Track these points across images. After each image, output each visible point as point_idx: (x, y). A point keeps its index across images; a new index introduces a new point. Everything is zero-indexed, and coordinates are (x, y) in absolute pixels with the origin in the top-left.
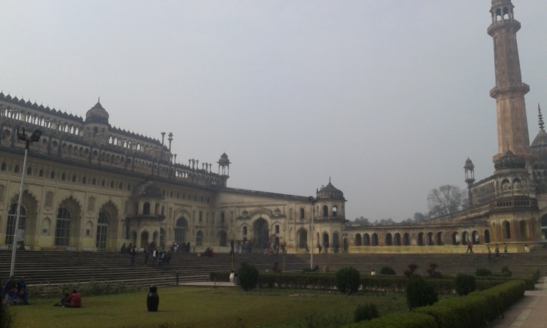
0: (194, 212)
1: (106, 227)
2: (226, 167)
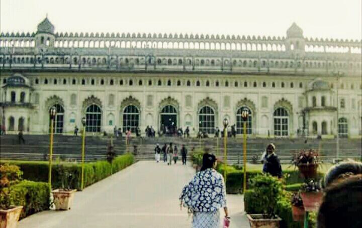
1: (287, 119)
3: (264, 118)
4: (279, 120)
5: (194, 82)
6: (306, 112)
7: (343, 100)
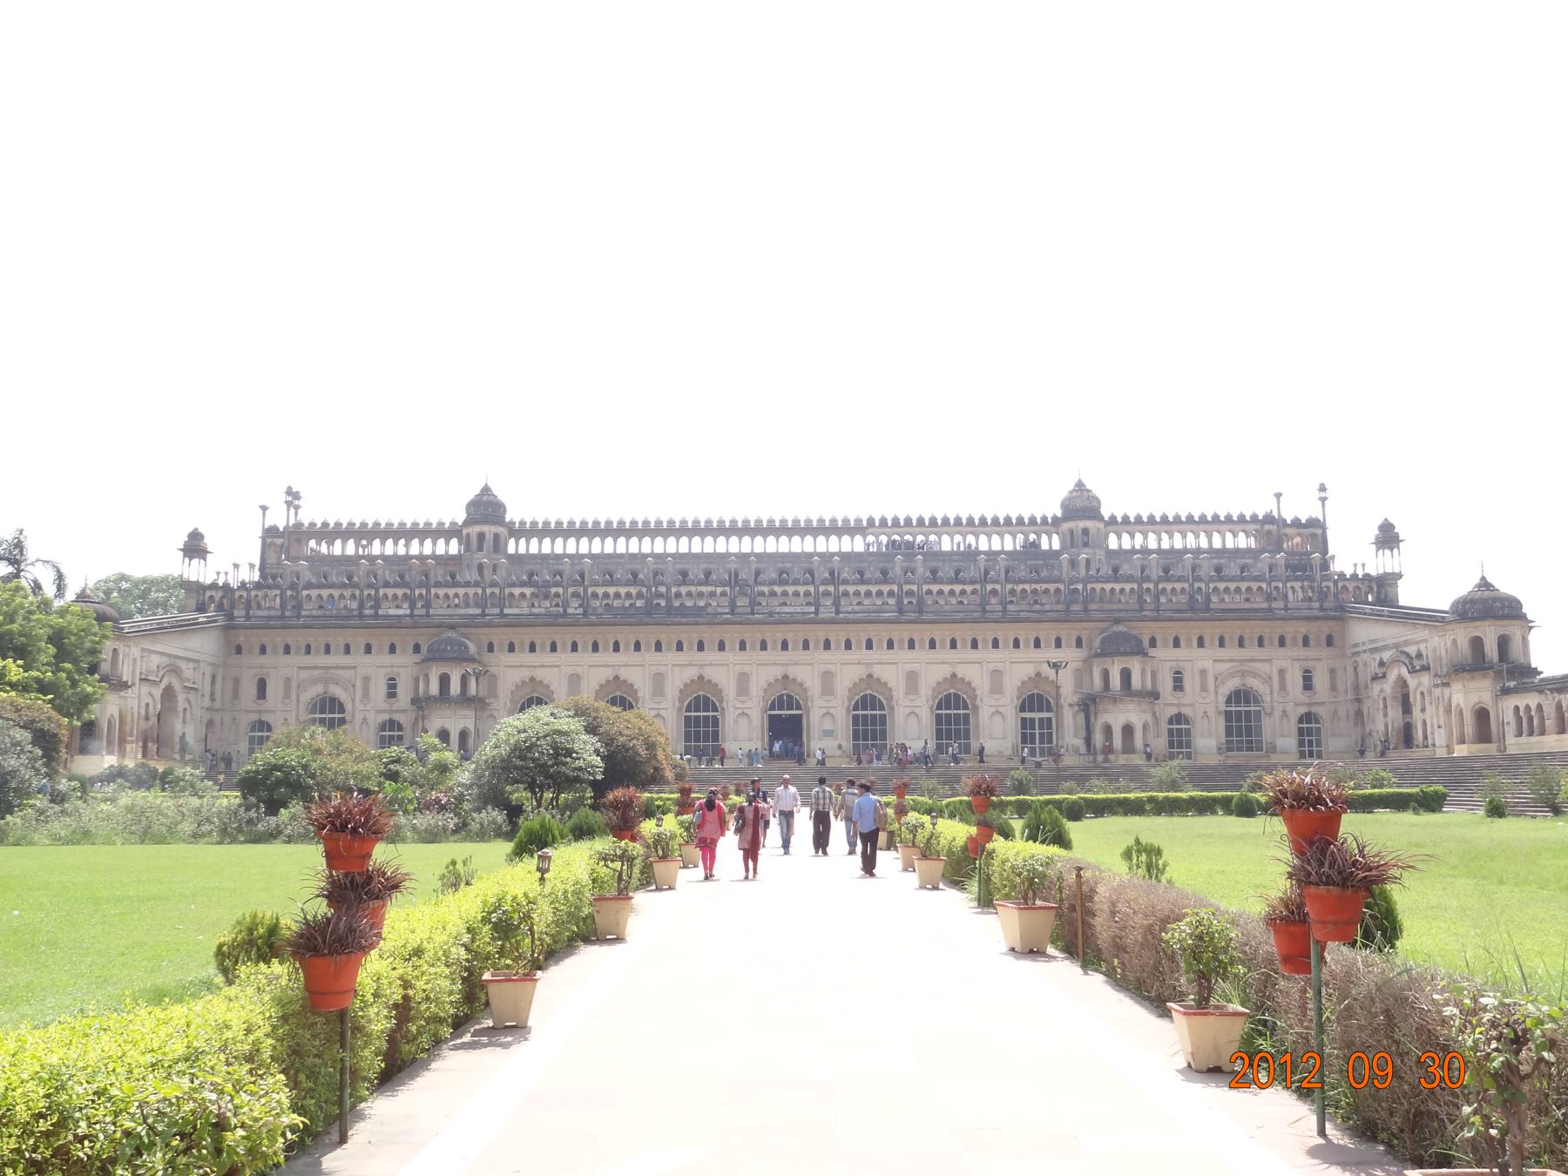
0: (1282, 672)
1: (1049, 720)
2: (1387, 552)
3: (998, 718)
4: (1032, 720)
5: (564, 645)
6: (1088, 705)
7: (1178, 672)
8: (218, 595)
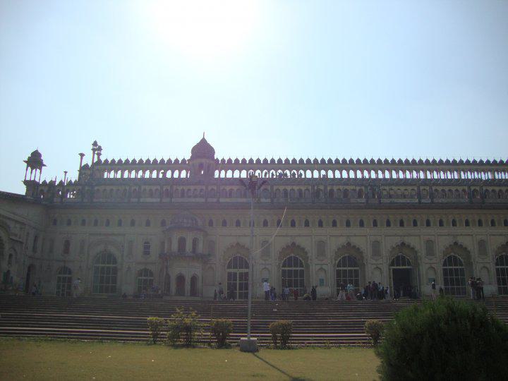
8: (46, 189)
